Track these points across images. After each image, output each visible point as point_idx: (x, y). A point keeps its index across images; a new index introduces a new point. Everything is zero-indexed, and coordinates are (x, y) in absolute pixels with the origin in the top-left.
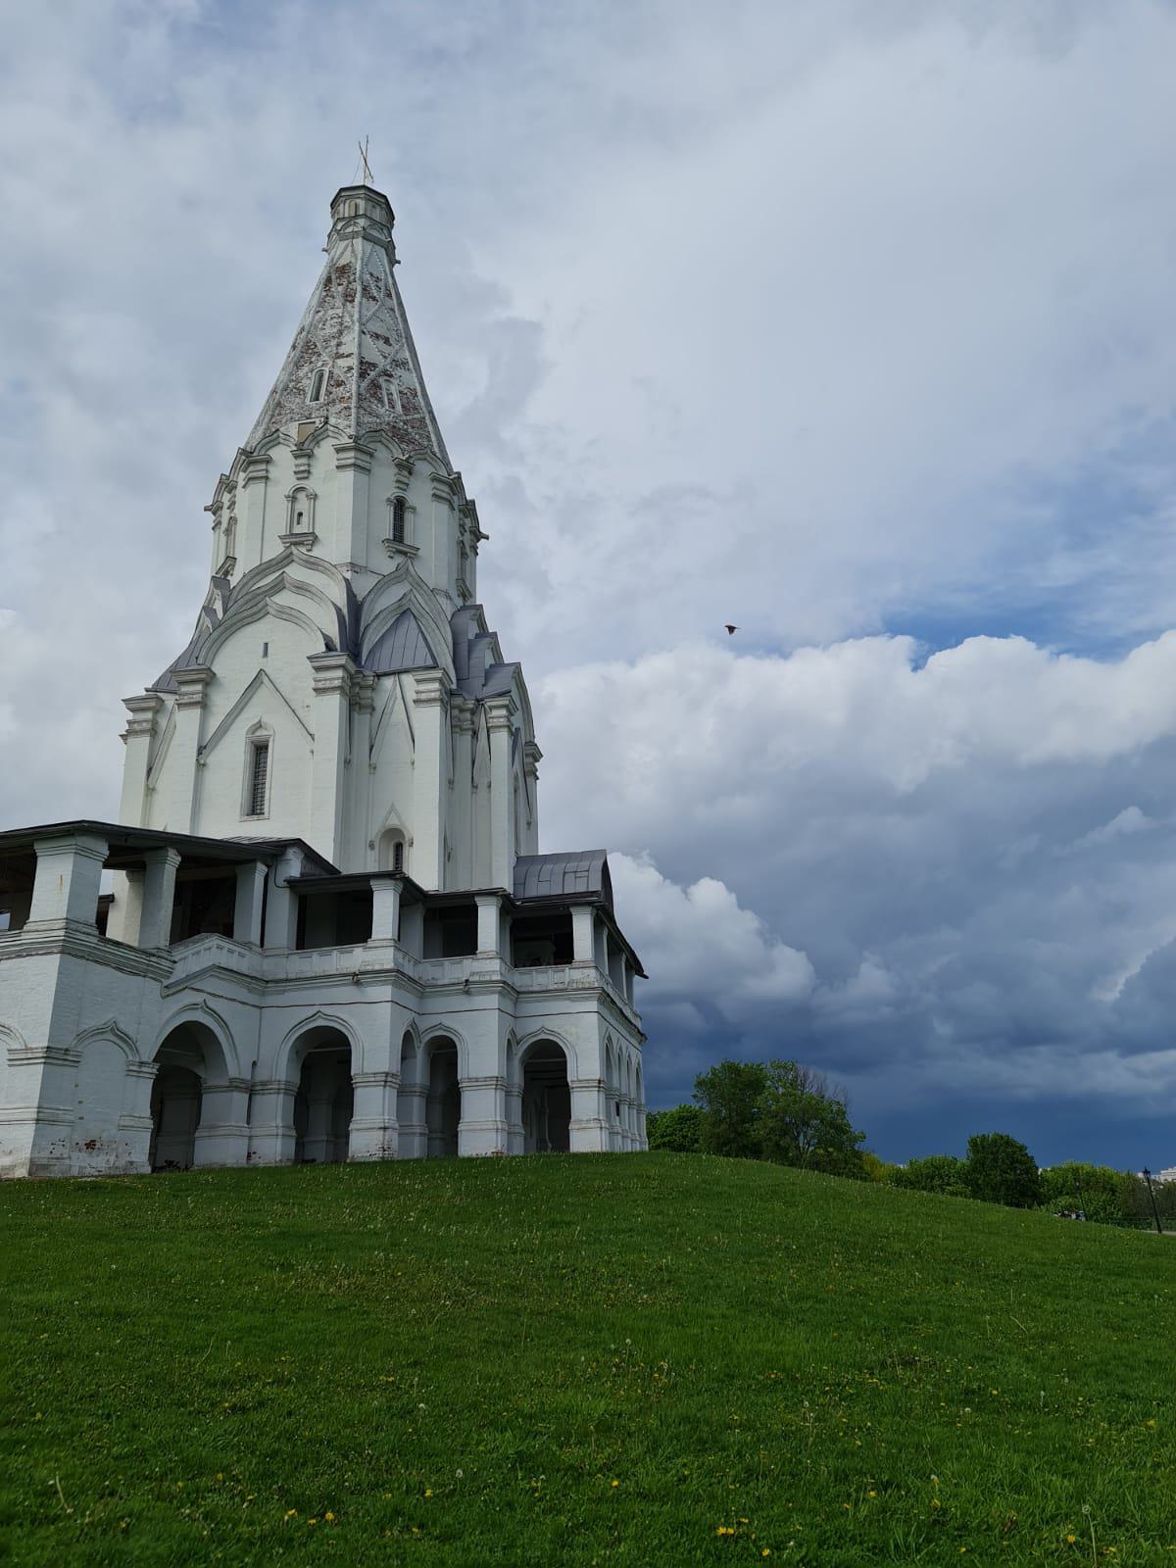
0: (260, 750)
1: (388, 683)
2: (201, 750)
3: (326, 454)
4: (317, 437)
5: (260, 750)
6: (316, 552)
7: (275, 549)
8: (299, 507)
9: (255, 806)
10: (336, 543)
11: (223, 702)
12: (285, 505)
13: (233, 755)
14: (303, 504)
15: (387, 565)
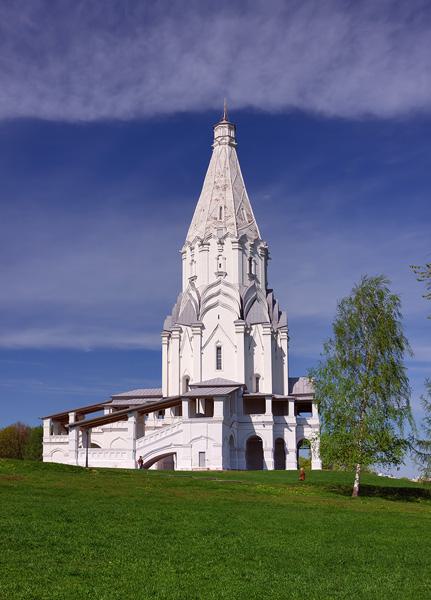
0: (219, 349)
1: (253, 327)
2: (201, 348)
3: (228, 241)
4: (225, 237)
5: (219, 349)
6: (227, 279)
7: (215, 279)
8: (220, 262)
9: (219, 367)
10: (233, 277)
11: (206, 333)
12: (216, 261)
13: (211, 351)
14: (221, 261)
15: (249, 284)
